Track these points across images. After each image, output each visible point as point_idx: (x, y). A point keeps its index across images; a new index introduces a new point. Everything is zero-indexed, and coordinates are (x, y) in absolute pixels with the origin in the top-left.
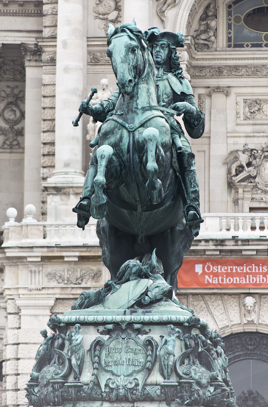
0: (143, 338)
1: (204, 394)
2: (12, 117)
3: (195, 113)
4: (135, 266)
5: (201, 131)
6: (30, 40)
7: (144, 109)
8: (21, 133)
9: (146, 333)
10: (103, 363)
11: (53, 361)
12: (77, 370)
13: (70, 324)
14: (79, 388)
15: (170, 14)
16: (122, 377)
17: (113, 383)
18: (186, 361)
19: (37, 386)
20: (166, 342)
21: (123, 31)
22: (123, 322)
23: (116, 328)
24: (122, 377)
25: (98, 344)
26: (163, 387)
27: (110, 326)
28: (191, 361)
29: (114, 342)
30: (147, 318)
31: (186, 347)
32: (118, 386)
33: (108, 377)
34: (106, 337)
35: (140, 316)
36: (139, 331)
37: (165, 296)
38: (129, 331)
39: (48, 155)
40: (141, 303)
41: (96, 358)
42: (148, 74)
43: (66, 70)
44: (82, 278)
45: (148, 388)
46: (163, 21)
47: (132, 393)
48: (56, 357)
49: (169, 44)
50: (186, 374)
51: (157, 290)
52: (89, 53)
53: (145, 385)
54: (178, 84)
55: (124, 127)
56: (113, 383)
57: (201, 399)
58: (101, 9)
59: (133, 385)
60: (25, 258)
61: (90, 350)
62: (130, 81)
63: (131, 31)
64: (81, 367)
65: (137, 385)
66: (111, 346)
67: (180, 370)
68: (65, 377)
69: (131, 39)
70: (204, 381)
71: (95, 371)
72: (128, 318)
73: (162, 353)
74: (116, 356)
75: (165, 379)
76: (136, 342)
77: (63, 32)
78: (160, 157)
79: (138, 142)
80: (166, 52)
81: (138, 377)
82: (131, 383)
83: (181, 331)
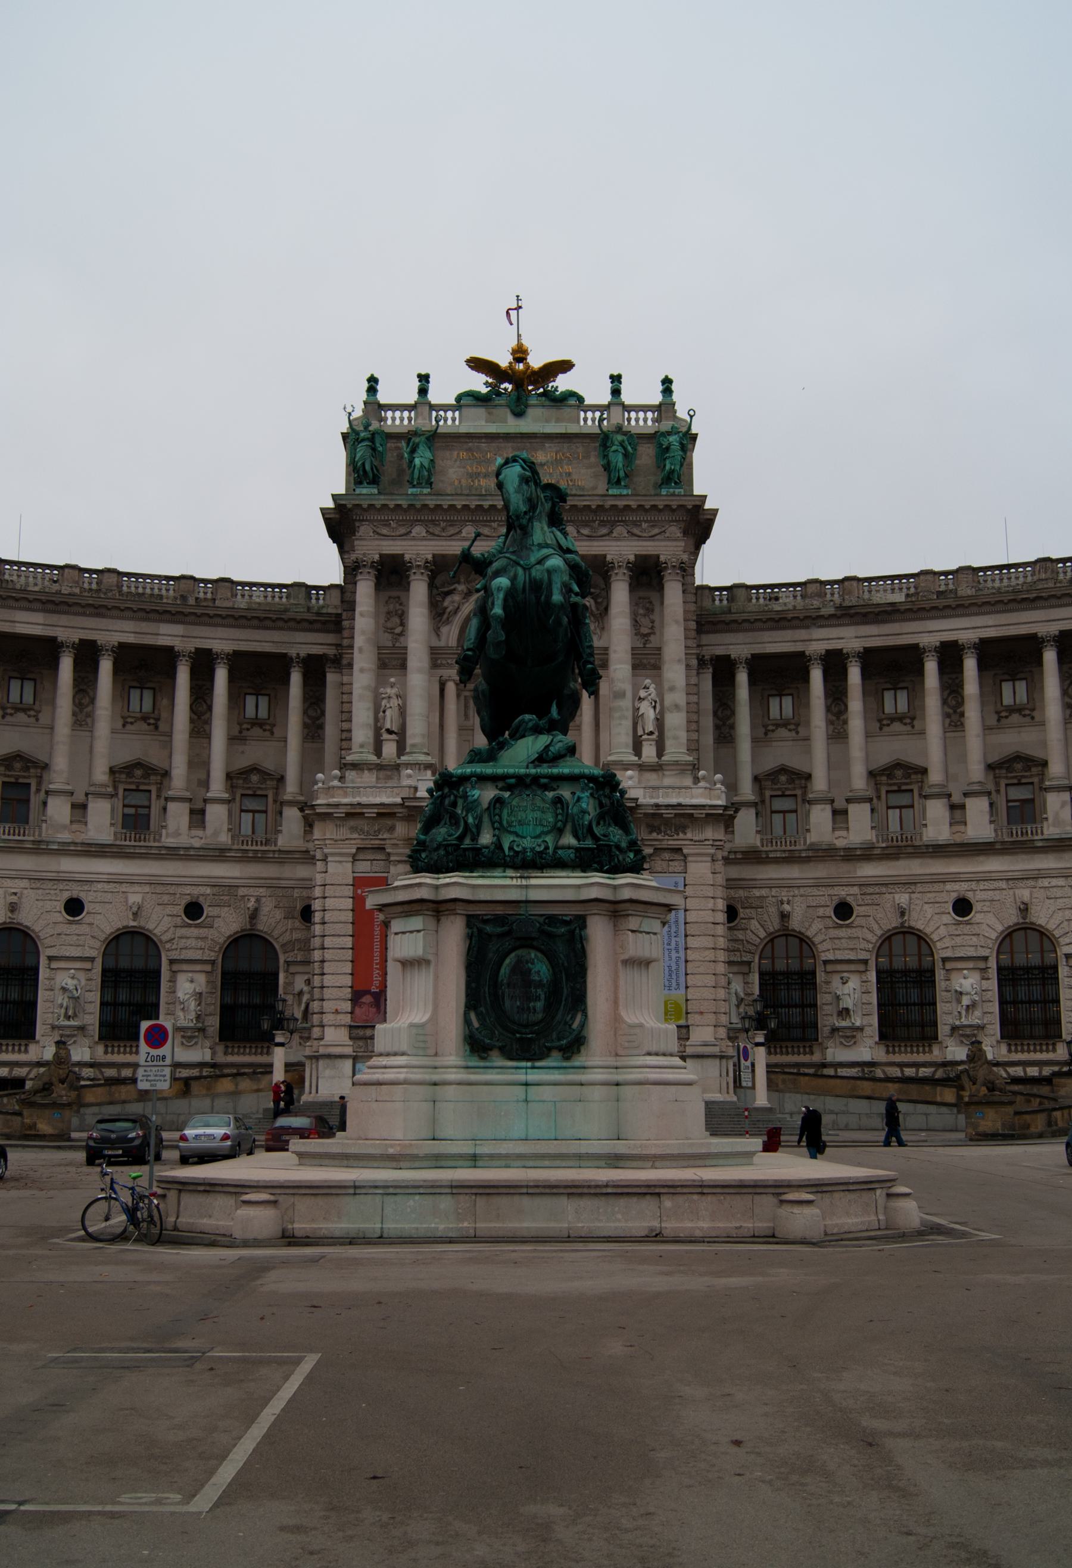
0: (550, 795)
2: (314, 714)
4: (531, 720)
6: (331, 652)
7: (541, 546)
8: (321, 727)
9: (554, 790)
10: (505, 823)
11: (443, 822)
12: (474, 830)
13: (464, 779)
14: (477, 851)
15: (444, 630)
16: (529, 838)
17: (518, 846)
19: (424, 851)
20: (579, 799)
21: (515, 461)
22: (527, 775)
23: (519, 784)
24: (529, 838)
25: (498, 801)
26: (577, 850)
27: (513, 781)
29: (517, 799)
30: (555, 771)
31: (601, 805)
32: (524, 849)
33: (512, 839)
34: (507, 794)
35: (545, 770)
36: (546, 788)
38: (534, 787)
39: (346, 740)
40: (542, 759)
41: (497, 818)
43: (362, 670)
44: (379, 831)
45: (560, 852)
46: (438, 635)
47: (541, 857)
48: (447, 817)
50: (604, 836)
51: (560, 744)
52: (379, 659)
53: (556, 848)
55: (518, 564)
56: (518, 846)
58: (389, 625)
59: (542, 848)
60: (332, 813)
61: (488, 808)
62: (525, 513)
64: (479, 827)
65: (547, 848)
66: (514, 803)
67: (598, 831)
68: (461, 838)
70: (624, 845)
71: (497, 832)
72: (533, 771)
73: (575, 810)
74: (521, 815)
75: (579, 840)
76: (543, 800)
77: (359, 641)
79: (535, 580)
80: (550, 504)
81: (547, 839)
82: (539, 846)
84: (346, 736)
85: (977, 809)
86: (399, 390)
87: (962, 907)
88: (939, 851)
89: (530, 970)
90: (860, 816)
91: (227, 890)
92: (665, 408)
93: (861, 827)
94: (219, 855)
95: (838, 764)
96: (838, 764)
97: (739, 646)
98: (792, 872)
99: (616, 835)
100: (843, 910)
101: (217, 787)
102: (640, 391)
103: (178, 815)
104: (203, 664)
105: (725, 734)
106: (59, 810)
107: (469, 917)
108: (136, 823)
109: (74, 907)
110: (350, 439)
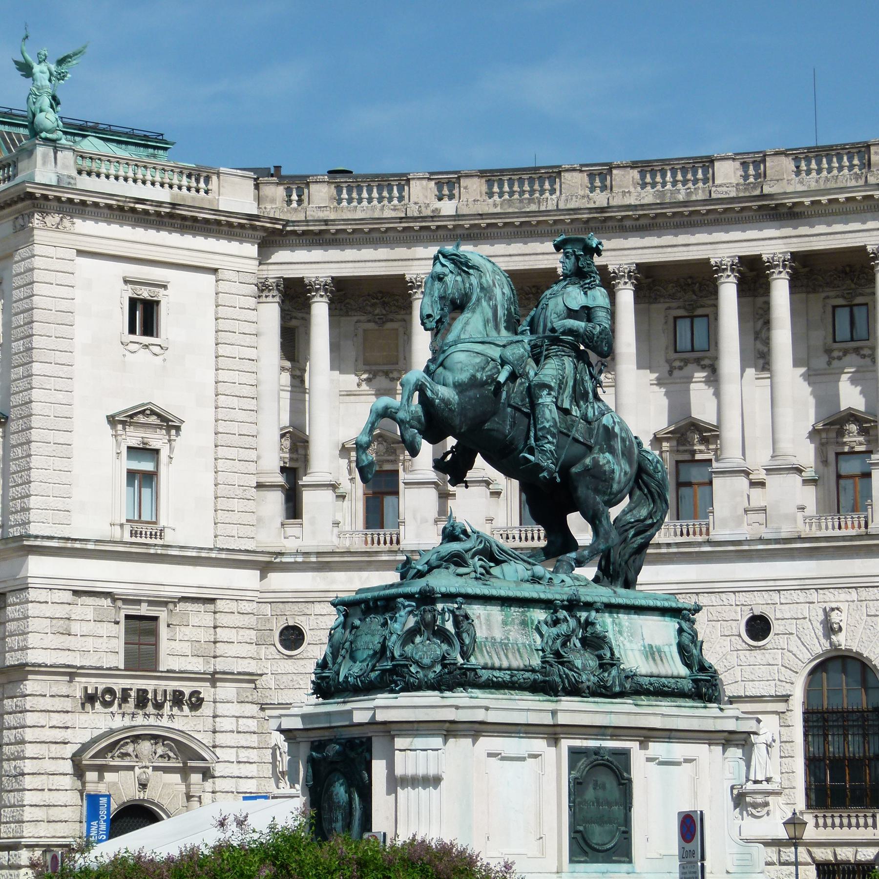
1: (425, 676)
3: (581, 330)
5: (606, 349)
18: (418, 639)
28: (426, 638)
37: (445, 561)
42: (479, 300)
49: (574, 251)
54: (579, 297)
57: (420, 682)
62: (429, 316)
63: (445, 256)
69: (443, 265)
70: (426, 661)
78: (437, 401)
80: (573, 258)
83: (414, 604)
89: (332, 792)
99: (427, 650)
107: (312, 742)
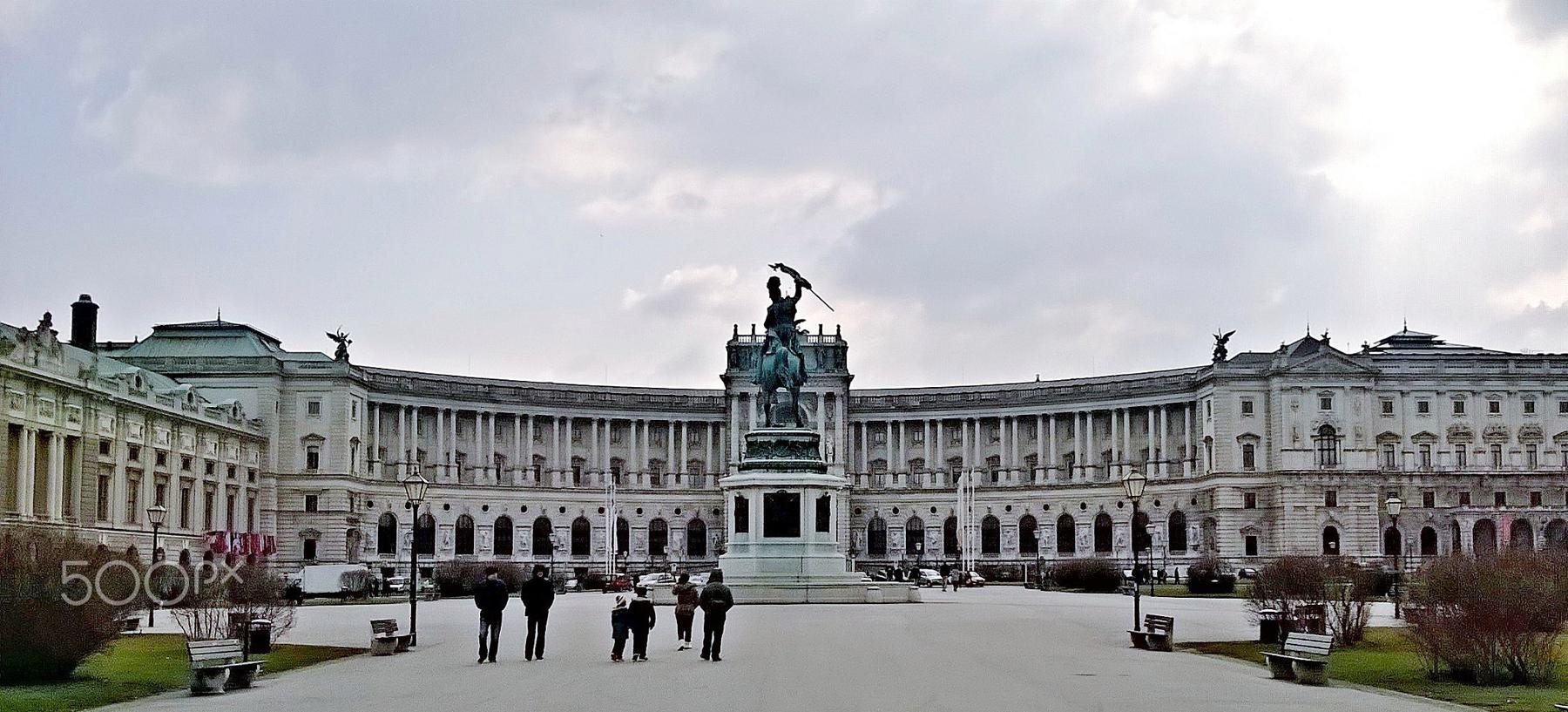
84: (728, 454)
85: (940, 477)
86: (745, 330)
87: (934, 510)
88: (926, 491)
90: (902, 478)
91: (689, 505)
92: (838, 336)
93: (902, 482)
94: (685, 492)
95: (896, 458)
96: (896, 458)
97: (863, 418)
98: (879, 497)
100: (896, 511)
101: (684, 469)
102: (830, 330)
103: (672, 478)
104: (678, 425)
105: (858, 445)
106: (633, 478)
108: (655, 481)
109: (639, 511)
110: (729, 348)
